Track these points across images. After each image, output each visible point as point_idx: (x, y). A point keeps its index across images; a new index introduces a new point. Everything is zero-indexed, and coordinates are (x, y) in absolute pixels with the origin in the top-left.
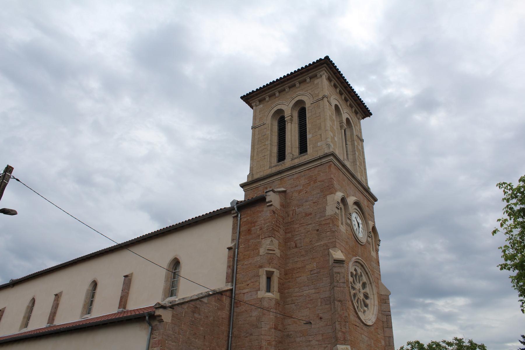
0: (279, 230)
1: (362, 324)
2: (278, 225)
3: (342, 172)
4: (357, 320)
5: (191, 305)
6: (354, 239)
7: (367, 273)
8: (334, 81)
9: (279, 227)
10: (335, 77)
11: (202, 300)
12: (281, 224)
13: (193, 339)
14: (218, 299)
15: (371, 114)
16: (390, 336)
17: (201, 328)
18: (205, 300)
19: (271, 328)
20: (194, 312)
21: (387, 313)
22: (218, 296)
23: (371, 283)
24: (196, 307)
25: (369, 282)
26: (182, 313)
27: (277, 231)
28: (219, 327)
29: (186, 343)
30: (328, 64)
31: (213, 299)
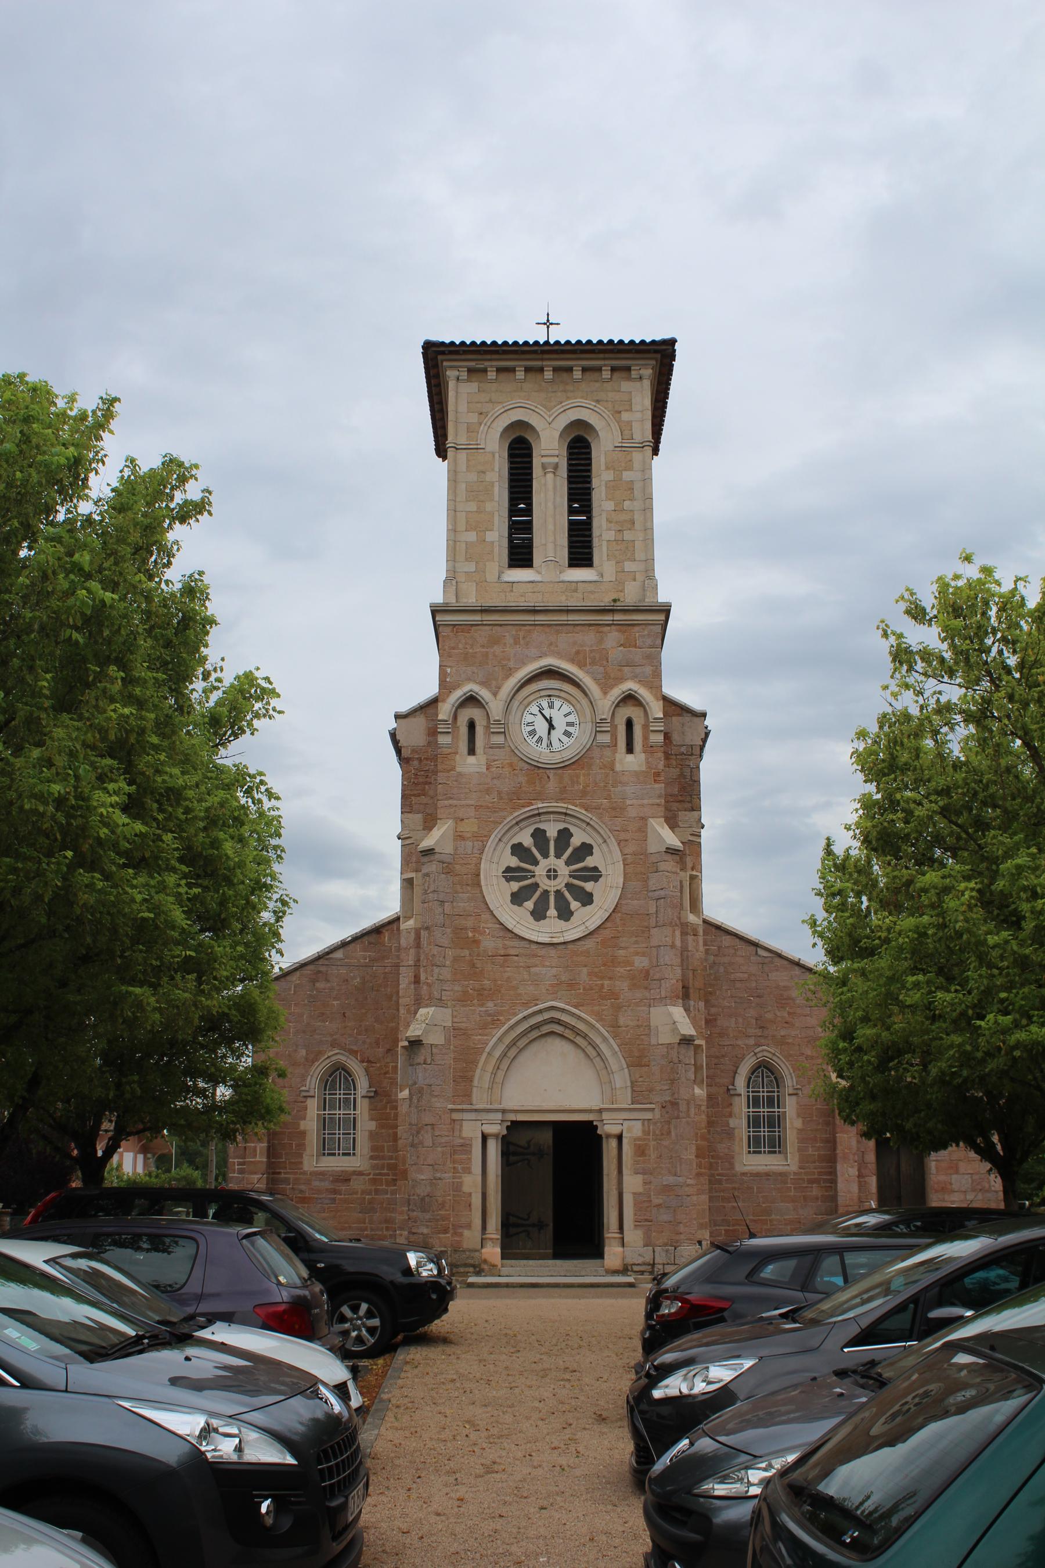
0: (424, 790)
1: (534, 946)
2: (421, 780)
3: (486, 625)
4: (516, 943)
5: (308, 971)
6: (526, 766)
7: (588, 824)
8: (492, 366)
9: (426, 783)
10: (488, 357)
11: (331, 956)
12: (430, 775)
13: (319, 1024)
14: (370, 943)
15: (672, 342)
16: (661, 944)
17: (335, 1003)
18: (339, 954)
19: (410, 983)
20: (314, 981)
21: (657, 893)
22: (373, 938)
23: (605, 841)
24: (319, 972)
25: (601, 841)
26: (290, 989)
27: (419, 795)
28: (378, 990)
29: (304, 1032)
30: (443, 353)
31: (358, 946)
